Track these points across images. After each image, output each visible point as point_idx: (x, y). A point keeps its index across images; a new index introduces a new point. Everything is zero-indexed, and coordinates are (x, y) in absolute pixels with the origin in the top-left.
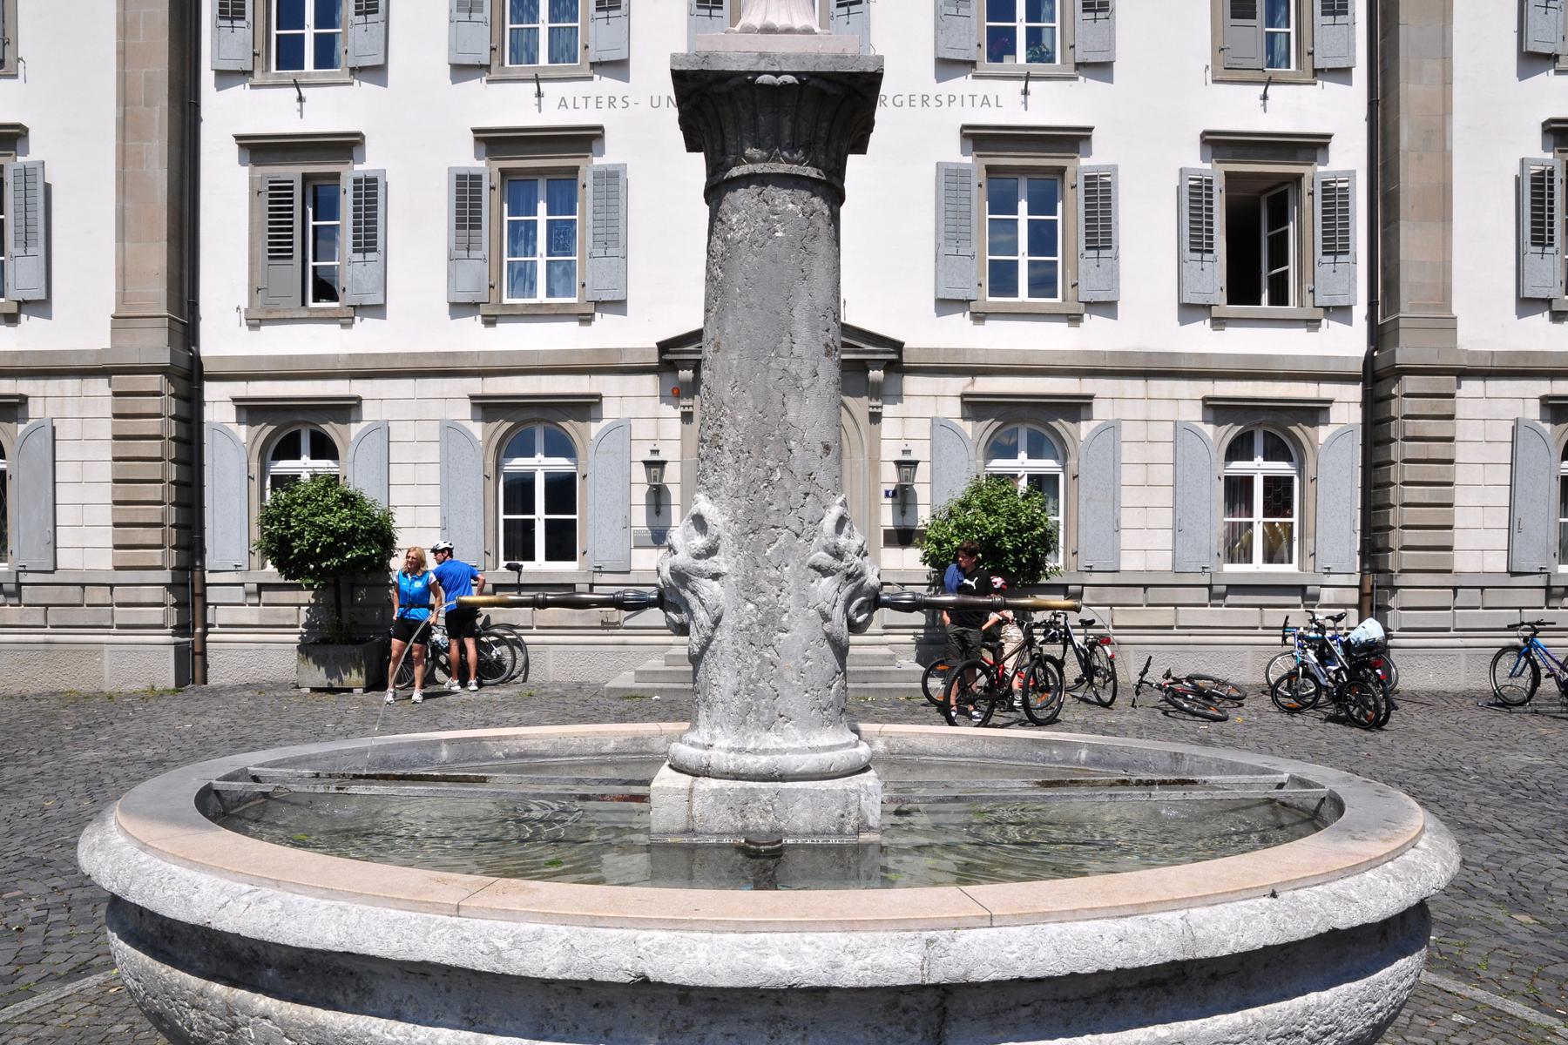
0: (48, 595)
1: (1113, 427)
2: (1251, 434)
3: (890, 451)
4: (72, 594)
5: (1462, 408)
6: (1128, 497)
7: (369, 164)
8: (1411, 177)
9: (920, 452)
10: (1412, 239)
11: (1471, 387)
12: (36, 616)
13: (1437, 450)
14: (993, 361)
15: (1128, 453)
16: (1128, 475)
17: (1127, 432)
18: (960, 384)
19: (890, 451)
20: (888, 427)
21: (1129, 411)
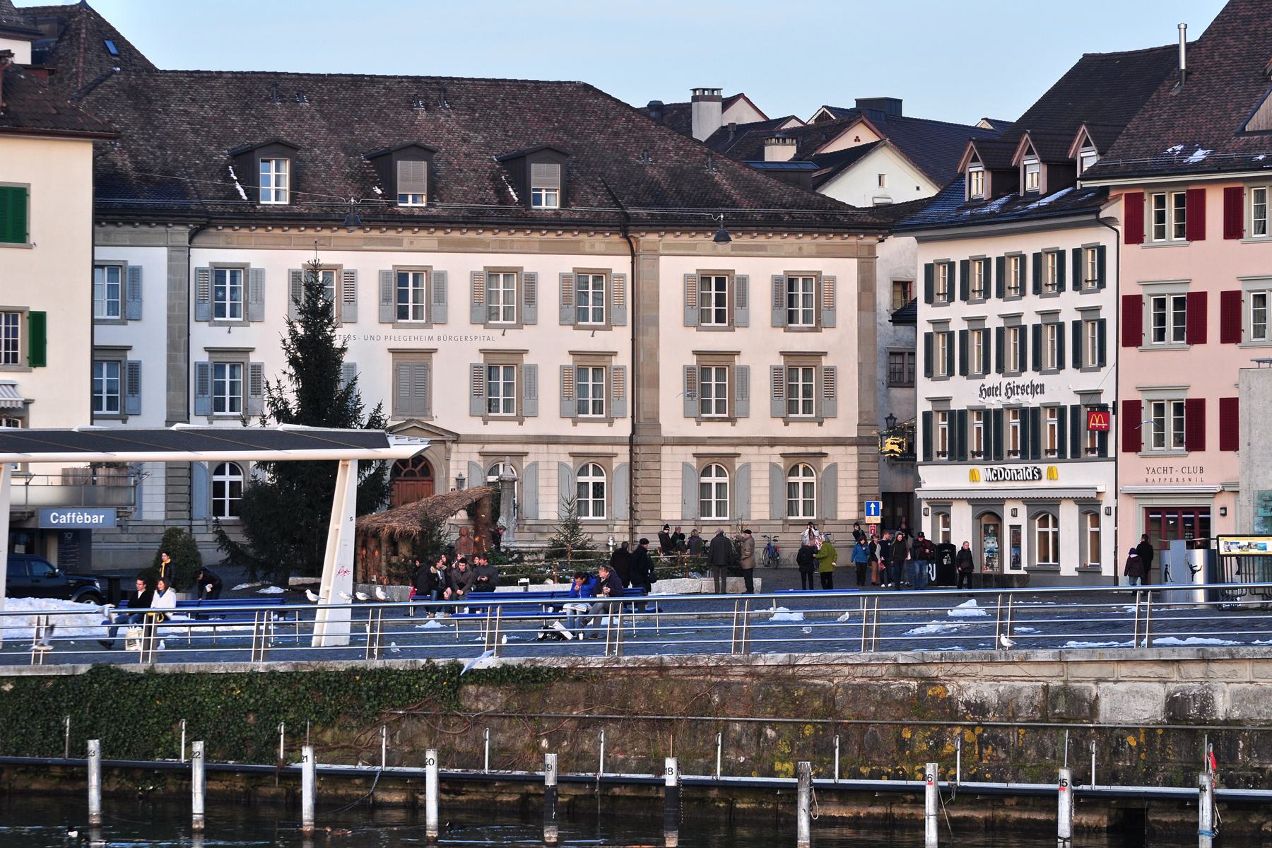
0: (141, 530)
1: (536, 464)
2: (587, 466)
3: (453, 474)
4: (148, 530)
5: (663, 458)
6: (541, 491)
7: (254, 358)
8: (645, 372)
9: (465, 476)
10: (645, 394)
11: (666, 450)
12: (133, 538)
13: (654, 474)
14: (491, 439)
15: (542, 474)
16: (541, 482)
17: (541, 466)
18: (477, 448)
19: (453, 474)
20: (452, 465)
21: (541, 458)
